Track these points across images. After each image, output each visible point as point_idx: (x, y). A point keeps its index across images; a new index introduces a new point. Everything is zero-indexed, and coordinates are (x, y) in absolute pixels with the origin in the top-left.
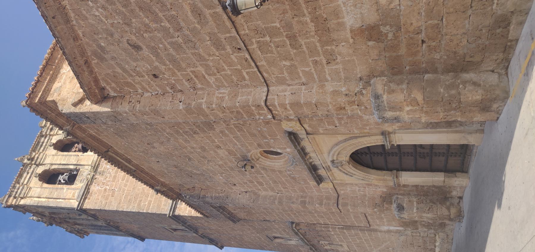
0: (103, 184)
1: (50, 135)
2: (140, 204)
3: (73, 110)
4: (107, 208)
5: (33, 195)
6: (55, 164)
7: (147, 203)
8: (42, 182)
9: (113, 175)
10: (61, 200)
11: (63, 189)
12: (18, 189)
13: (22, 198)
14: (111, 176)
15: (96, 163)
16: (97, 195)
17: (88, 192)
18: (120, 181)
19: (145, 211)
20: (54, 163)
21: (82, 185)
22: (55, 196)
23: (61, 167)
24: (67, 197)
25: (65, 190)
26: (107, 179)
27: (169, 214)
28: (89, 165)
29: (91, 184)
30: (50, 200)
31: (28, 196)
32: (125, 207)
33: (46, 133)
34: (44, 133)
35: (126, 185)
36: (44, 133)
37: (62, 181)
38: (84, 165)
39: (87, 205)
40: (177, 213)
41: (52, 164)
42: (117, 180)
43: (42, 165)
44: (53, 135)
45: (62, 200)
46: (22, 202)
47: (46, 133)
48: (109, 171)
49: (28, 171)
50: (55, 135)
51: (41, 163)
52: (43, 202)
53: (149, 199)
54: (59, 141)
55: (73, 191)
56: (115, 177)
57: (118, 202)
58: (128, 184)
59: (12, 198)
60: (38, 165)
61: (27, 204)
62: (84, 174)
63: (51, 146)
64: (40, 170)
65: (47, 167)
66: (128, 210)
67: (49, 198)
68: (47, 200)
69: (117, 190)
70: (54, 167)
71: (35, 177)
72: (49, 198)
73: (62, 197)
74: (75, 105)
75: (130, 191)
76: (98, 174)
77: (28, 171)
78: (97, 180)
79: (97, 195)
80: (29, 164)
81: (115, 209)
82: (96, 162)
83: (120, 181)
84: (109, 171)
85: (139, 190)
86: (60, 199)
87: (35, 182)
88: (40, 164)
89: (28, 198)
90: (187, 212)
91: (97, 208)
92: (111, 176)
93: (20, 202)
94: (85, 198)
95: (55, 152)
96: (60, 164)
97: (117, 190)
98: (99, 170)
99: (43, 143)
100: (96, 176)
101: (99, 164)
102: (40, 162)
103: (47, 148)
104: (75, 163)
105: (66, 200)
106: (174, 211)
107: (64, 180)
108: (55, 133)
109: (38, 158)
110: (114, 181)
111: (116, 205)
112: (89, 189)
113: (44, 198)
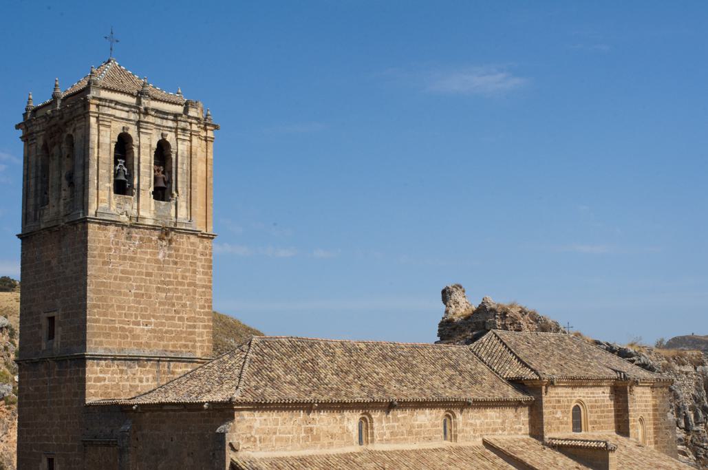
0: (117, 244)
1: (177, 129)
2: (96, 307)
3: (227, 443)
4: (89, 259)
5: (102, 133)
6: (139, 153)
7: (97, 317)
8: (116, 140)
9: (127, 255)
10: (96, 181)
11: (110, 183)
12: (109, 107)
13: (97, 118)
14: (126, 251)
15: (141, 224)
16: (103, 238)
17: (106, 225)
18: (121, 268)
19: (88, 317)
20: (141, 150)
21: (113, 207)
22: (100, 170)
23: (136, 163)
24: (100, 192)
25: (108, 185)
26: (122, 247)
27: (87, 355)
28: (138, 209)
29: (116, 225)
30: (96, 163)
31: (101, 128)
32: (91, 287)
33: (180, 121)
34: (179, 118)
35: (115, 278)
36: (179, 118)
37: (118, 168)
38: (138, 201)
39: (92, 229)
40: (89, 362)
41: (139, 147)
42: (122, 262)
43: (139, 132)
44: (176, 132)
45: (96, 185)
46: (93, 120)
47: (180, 121)
48: (131, 247)
49: (131, 111)
50: (176, 135)
51: (142, 130)
52: (94, 154)
53: (102, 318)
54: (167, 144)
55: (106, 198)
56: (124, 258)
57: (97, 275)
58: (118, 282)
59: (98, 102)
60: (138, 123)
61: (91, 129)
62: (128, 205)
63: (162, 135)
64: (132, 131)
65: (135, 142)
66: (88, 292)
67: (98, 163)
68: (96, 158)
69: (110, 267)
70: (135, 150)
71: (124, 128)
72: (98, 163)
73: (100, 183)
74: (231, 444)
75: (110, 287)
76: (128, 230)
77: (131, 111)
78: (121, 231)
79: (103, 238)
80: (139, 109)
81: (89, 273)
82: (144, 225)
83: (121, 268)
84: (131, 247)
85: (111, 299)
86: (98, 179)
87: (117, 127)
88: (139, 128)
89: (96, 125)
90: (90, 376)
91: (89, 244)
92: (126, 251)
93: (93, 117)
94: (99, 223)
95: (155, 145)
96: (139, 163)
97: (110, 267)
98: (133, 230)
99: (167, 119)
100: (125, 229)
101: (140, 228)
102: (142, 128)
103: (160, 129)
104: (141, 187)
105: (96, 191)
106: (90, 359)
107: (119, 170)
108: (179, 137)
109: (148, 123)
110: (120, 259)
111: (93, 273)
112: (111, 224)
113: (98, 153)
